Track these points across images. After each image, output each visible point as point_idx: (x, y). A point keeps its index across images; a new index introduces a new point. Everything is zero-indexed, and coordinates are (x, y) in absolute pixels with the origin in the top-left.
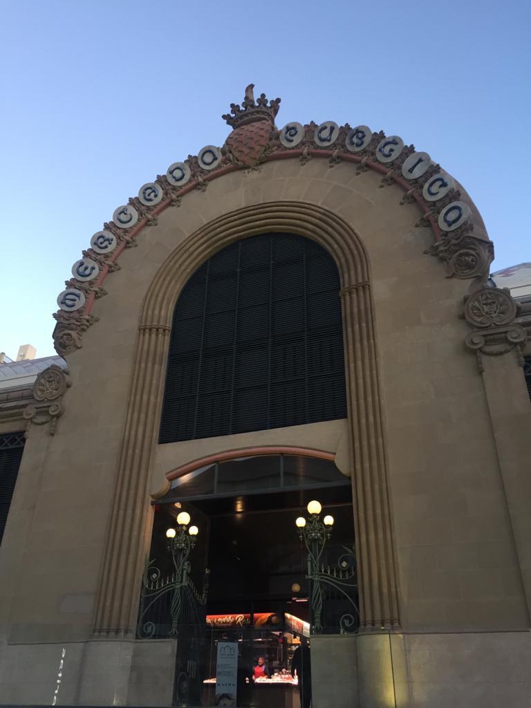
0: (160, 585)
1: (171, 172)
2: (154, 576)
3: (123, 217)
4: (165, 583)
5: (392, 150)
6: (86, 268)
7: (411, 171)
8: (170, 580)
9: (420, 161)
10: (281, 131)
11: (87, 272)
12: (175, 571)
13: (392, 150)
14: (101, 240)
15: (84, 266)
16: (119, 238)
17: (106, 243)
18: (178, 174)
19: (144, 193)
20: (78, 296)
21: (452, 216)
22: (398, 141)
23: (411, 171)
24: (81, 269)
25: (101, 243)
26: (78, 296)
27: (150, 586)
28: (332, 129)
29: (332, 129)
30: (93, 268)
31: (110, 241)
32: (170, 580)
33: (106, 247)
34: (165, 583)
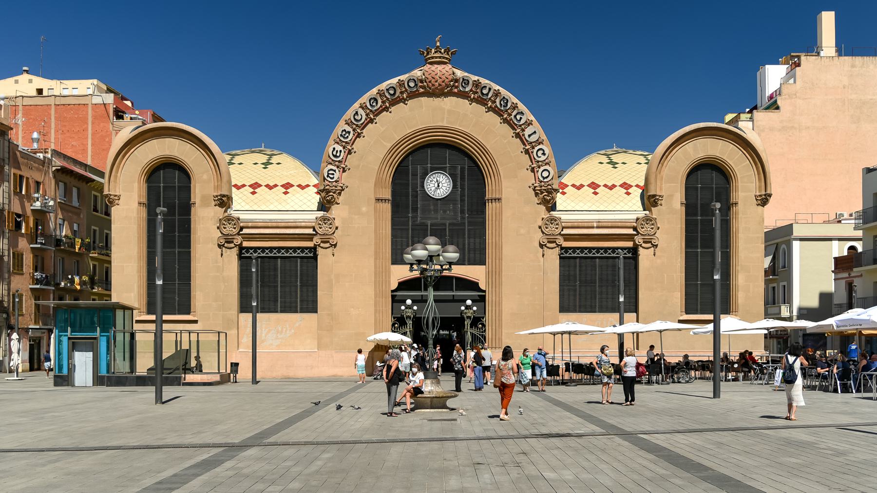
0: (400, 329)
1: (387, 90)
2: (396, 325)
3: (358, 118)
4: (402, 328)
5: (521, 118)
6: (337, 151)
7: (529, 136)
8: (404, 327)
9: (535, 132)
10: (460, 78)
11: (338, 155)
12: (407, 324)
13: (521, 118)
14: (344, 133)
15: (339, 151)
16: (354, 130)
17: (347, 135)
18: (392, 92)
19: (370, 101)
20: (335, 171)
21: (545, 174)
22: (524, 113)
23: (529, 136)
24: (335, 153)
25: (344, 135)
26: (335, 171)
27: (395, 329)
28: (490, 89)
29: (490, 89)
30: (341, 151)
31: (349, 133)
32: (404, 327)
33: (348, 137)
34: (402, 328)
